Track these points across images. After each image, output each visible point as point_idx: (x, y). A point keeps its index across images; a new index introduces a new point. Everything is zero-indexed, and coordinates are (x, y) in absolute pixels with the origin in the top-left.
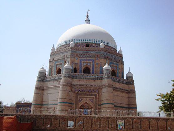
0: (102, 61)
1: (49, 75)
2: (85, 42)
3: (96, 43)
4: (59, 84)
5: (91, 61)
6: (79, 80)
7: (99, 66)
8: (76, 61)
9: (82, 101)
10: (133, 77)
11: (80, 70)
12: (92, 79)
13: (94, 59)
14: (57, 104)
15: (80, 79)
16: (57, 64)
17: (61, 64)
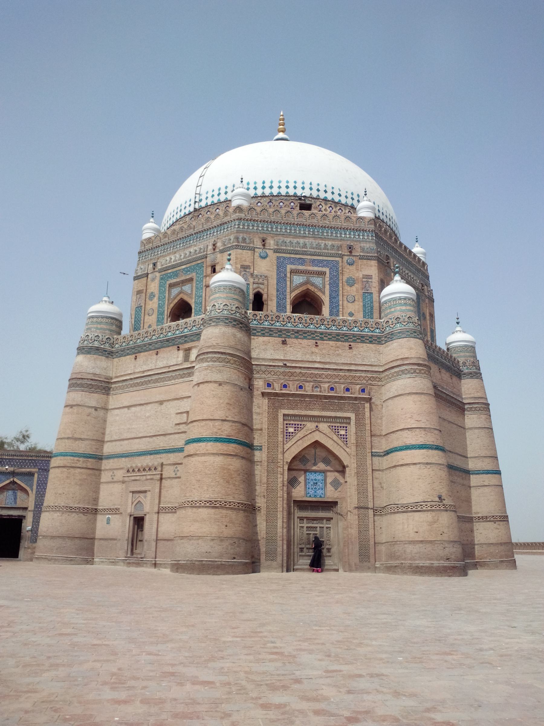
0: (372, 269)
1: (136, 327)
2: (295, 195)
3: (339, 203)
4: (186, 358)
5: (324, 269)
6: (280, 339)
7: (357, 291)
9: (300, 435)
10: (474, 348)
11: (278, 302)
12: (337, 337)
13: (337, 259)
14: (181, 450)
15: (284, 336)
16: (168, 283)
17: (191, 280)
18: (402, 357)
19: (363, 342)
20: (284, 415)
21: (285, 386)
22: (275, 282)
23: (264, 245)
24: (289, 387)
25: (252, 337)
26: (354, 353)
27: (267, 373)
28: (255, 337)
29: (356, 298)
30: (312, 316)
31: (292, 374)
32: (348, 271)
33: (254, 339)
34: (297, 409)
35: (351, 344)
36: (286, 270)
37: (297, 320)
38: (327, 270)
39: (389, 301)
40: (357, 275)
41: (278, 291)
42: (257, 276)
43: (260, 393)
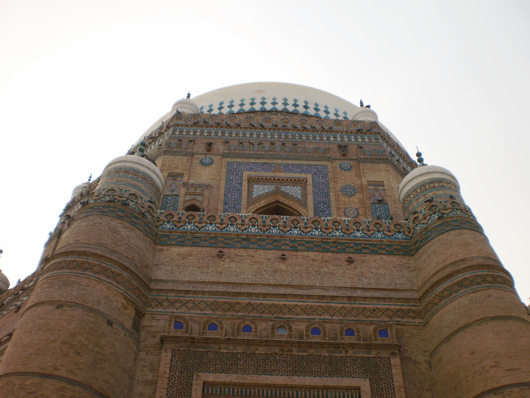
5: (303, 175)
6: (215, 251)
7: (362, 202)
8: (204, 175)
13: (324, 163)
18: (453, 260)
19: (375, 253)
20: (205, 384)
21: (213, 327)
22: (222, 191)
23: (209, 150)
24: (222, 328)
25: (159, 247)
26: (359, 270)
27: (177, 305)
28: (164, 248)
29: (361, 211)
30: (276, 217)
31: (231, 307)
32: (343, 178)
33: (161, 250)
34: (236, 372)
35: (352, 256)
36: (241, 178)
37: (247, 221)
38: (309, 177)
39: (414, 190)
40: (359, 182)
41: (226, 203)
42: (192, 185)
43: (157, 340)
